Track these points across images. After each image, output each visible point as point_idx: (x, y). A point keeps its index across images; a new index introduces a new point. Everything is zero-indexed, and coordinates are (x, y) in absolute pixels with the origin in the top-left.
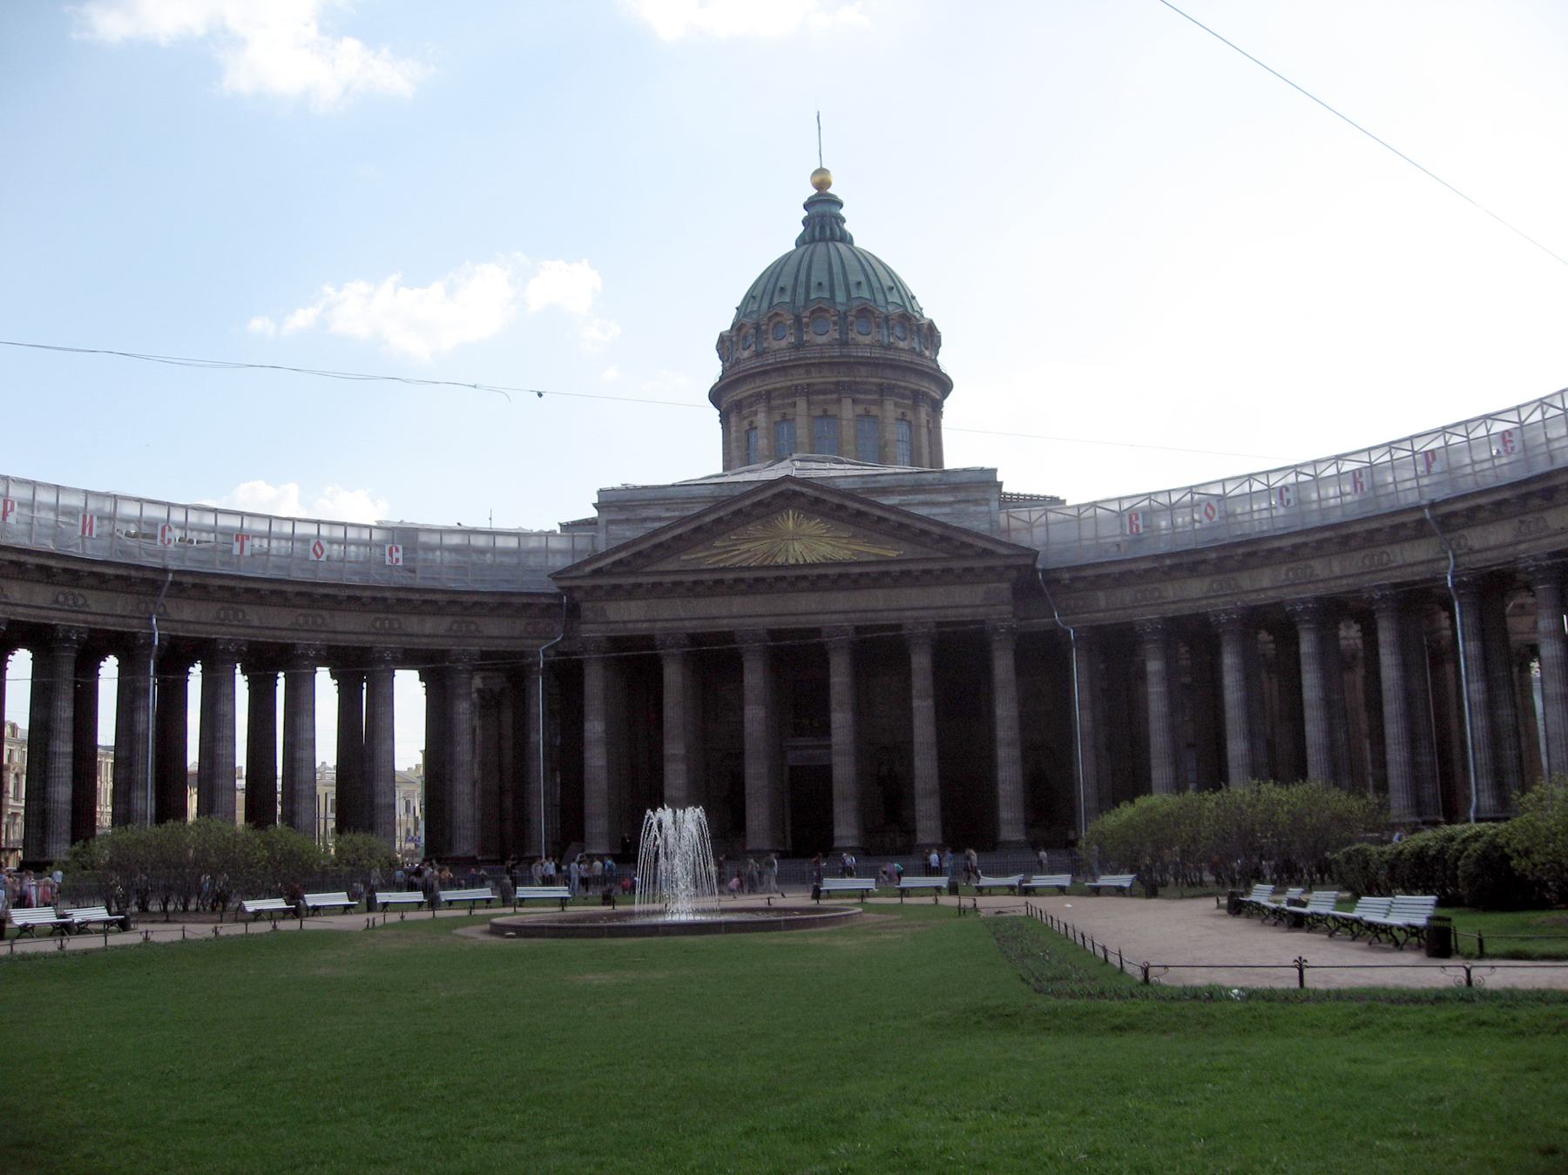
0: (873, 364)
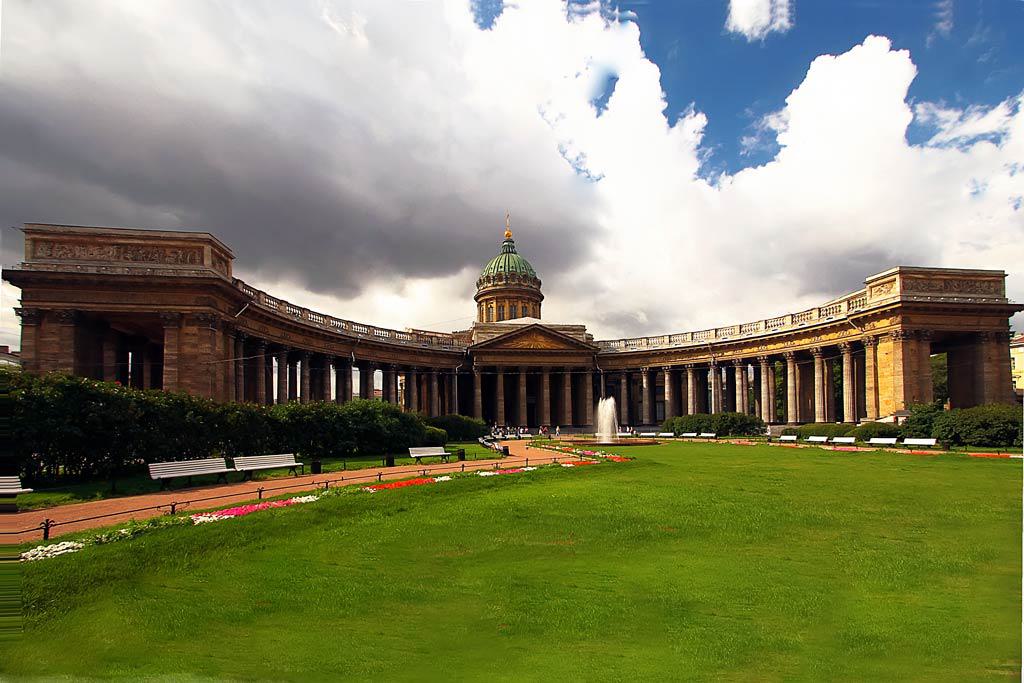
0: (527, 292)
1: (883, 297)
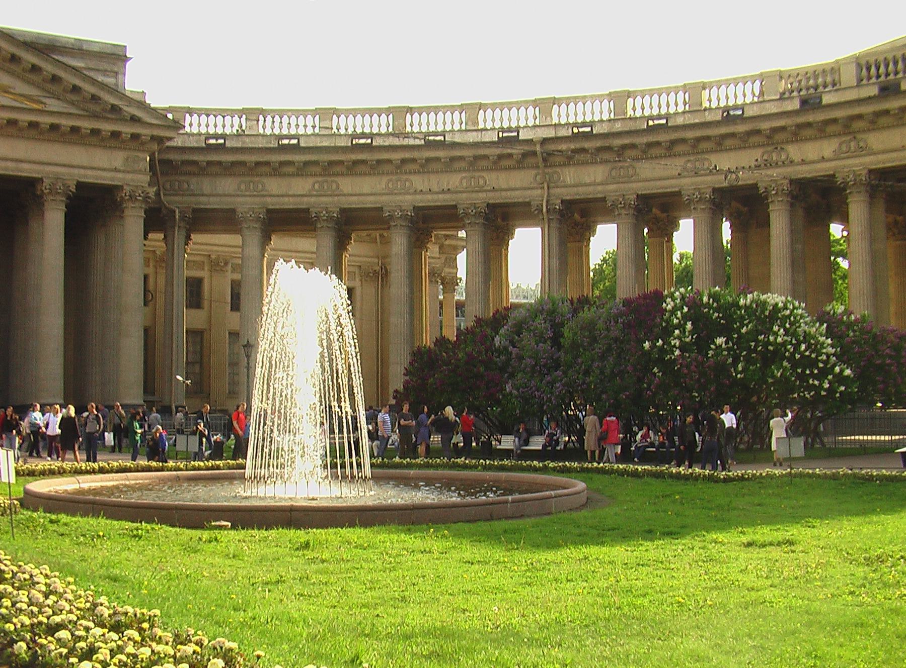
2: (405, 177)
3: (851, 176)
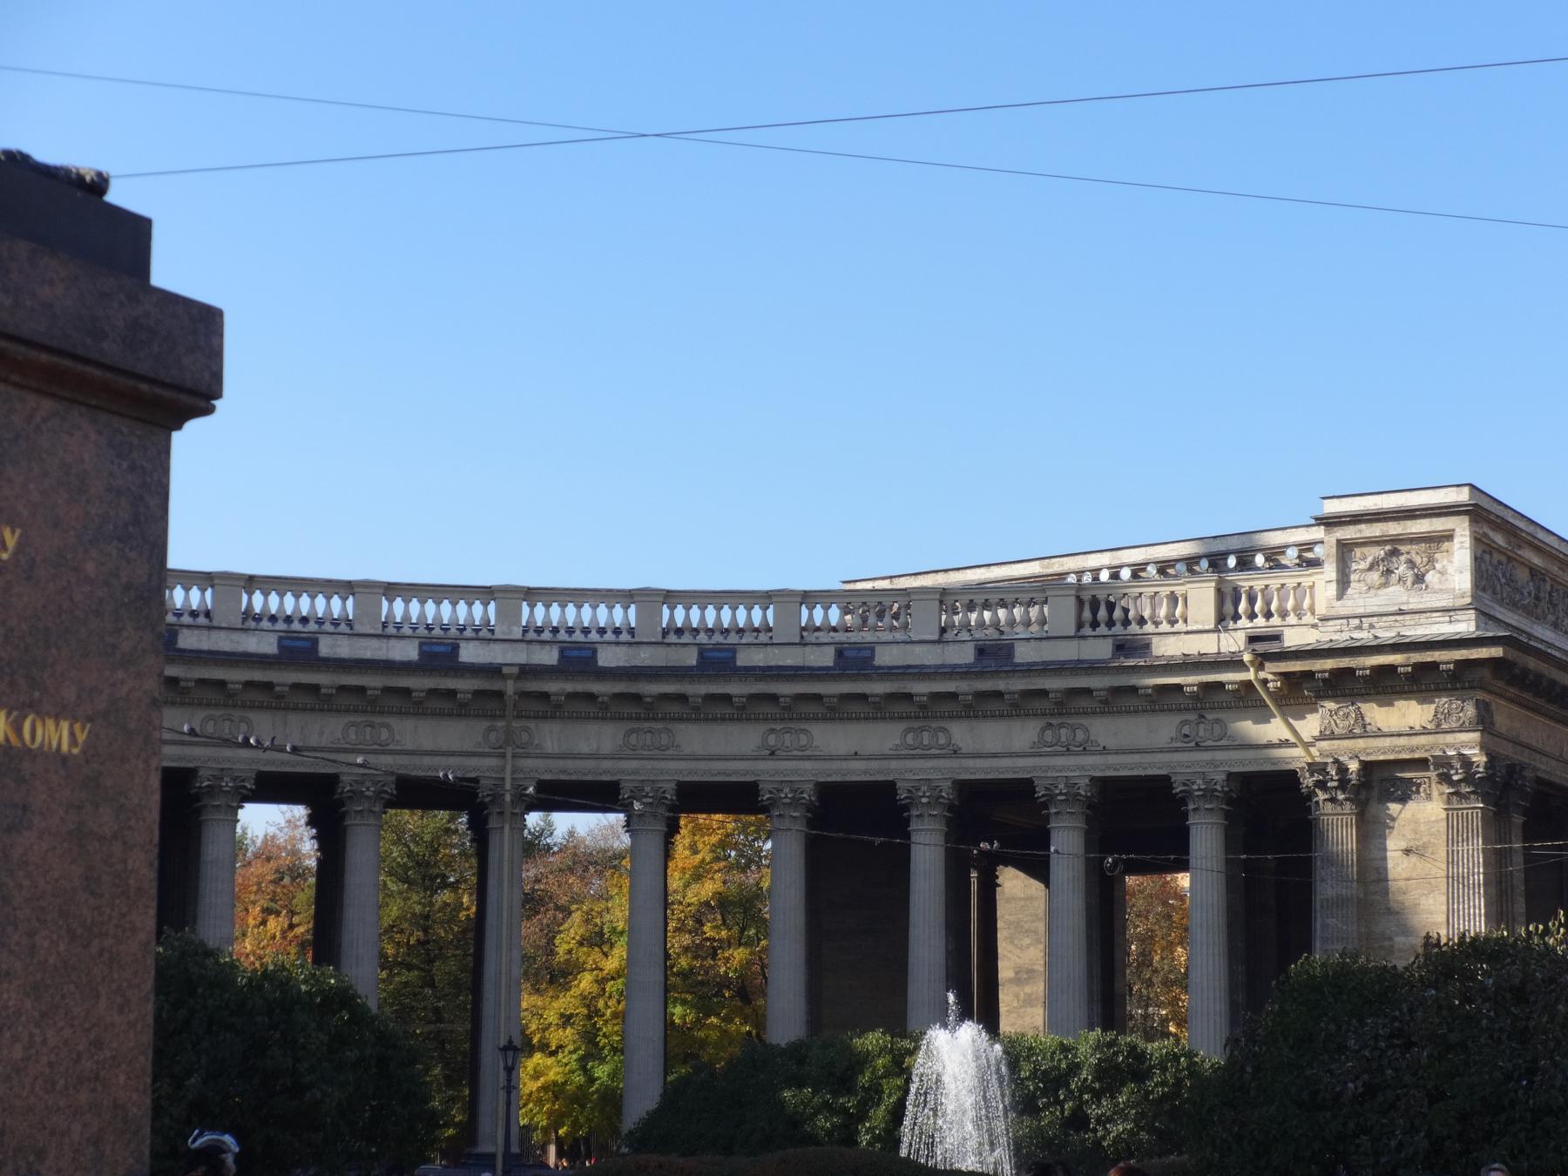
1: (1398, 595)
2: (237, 714)
3: (1061, 786)
